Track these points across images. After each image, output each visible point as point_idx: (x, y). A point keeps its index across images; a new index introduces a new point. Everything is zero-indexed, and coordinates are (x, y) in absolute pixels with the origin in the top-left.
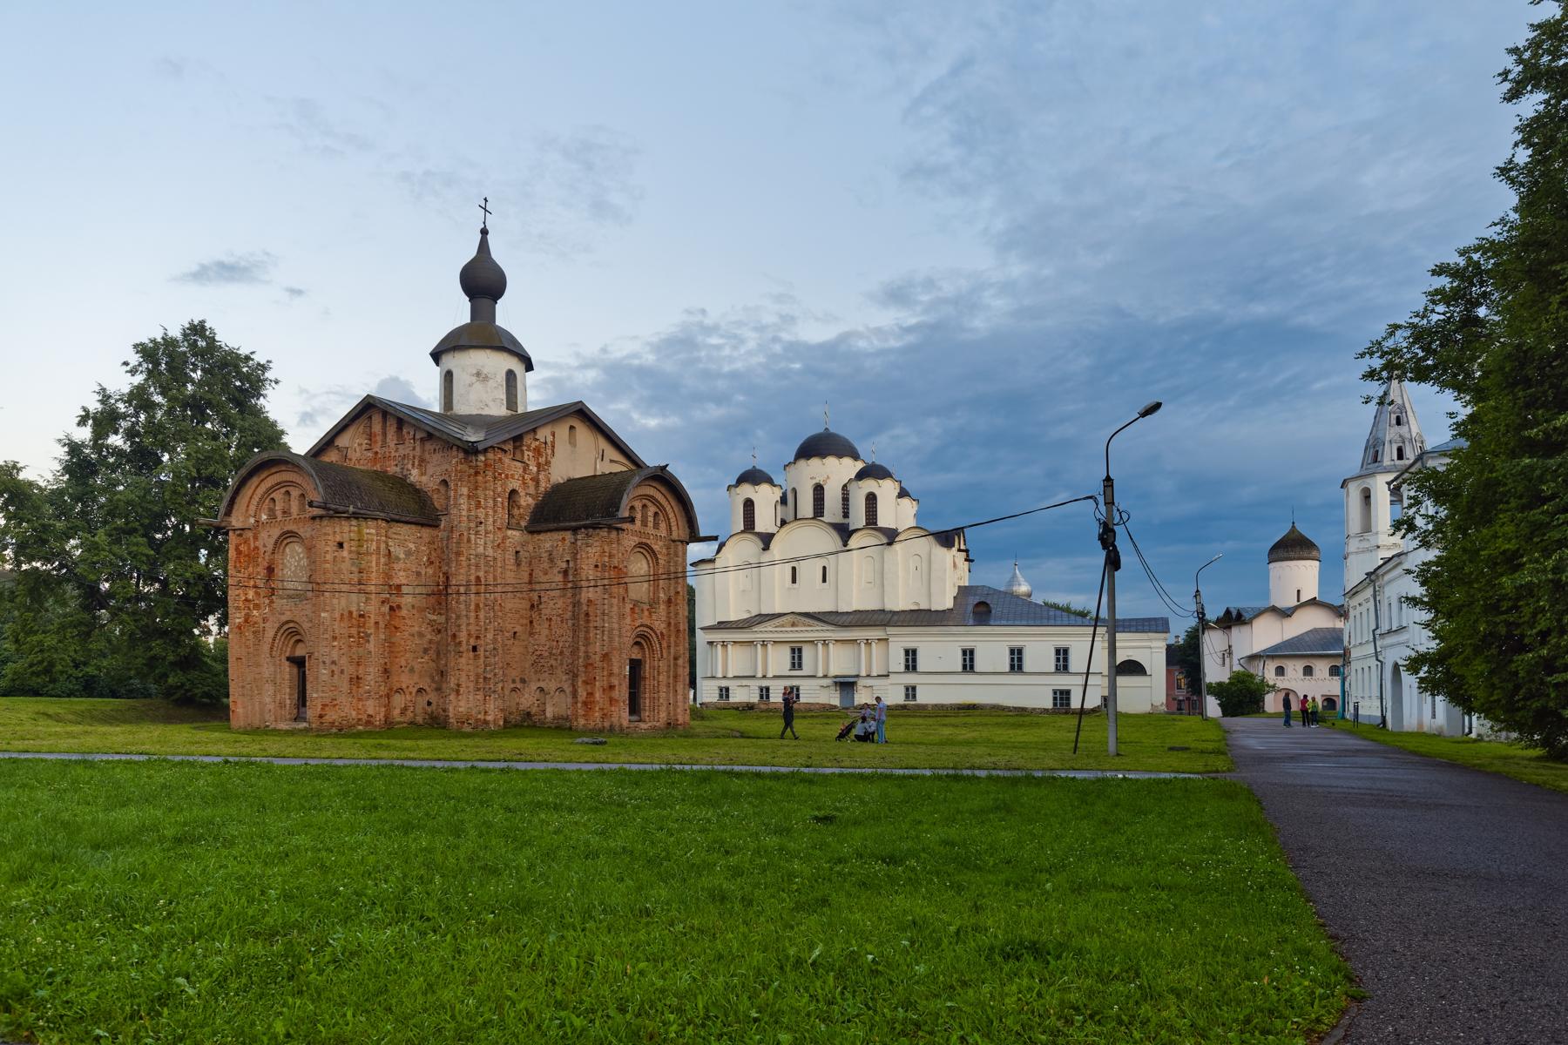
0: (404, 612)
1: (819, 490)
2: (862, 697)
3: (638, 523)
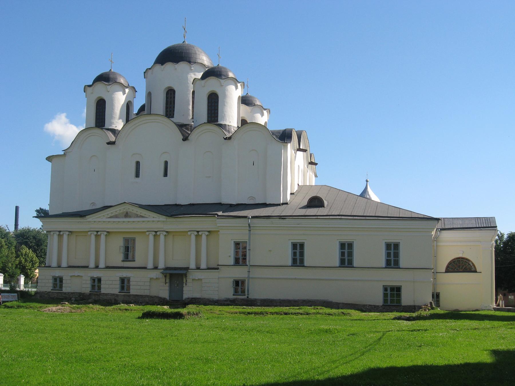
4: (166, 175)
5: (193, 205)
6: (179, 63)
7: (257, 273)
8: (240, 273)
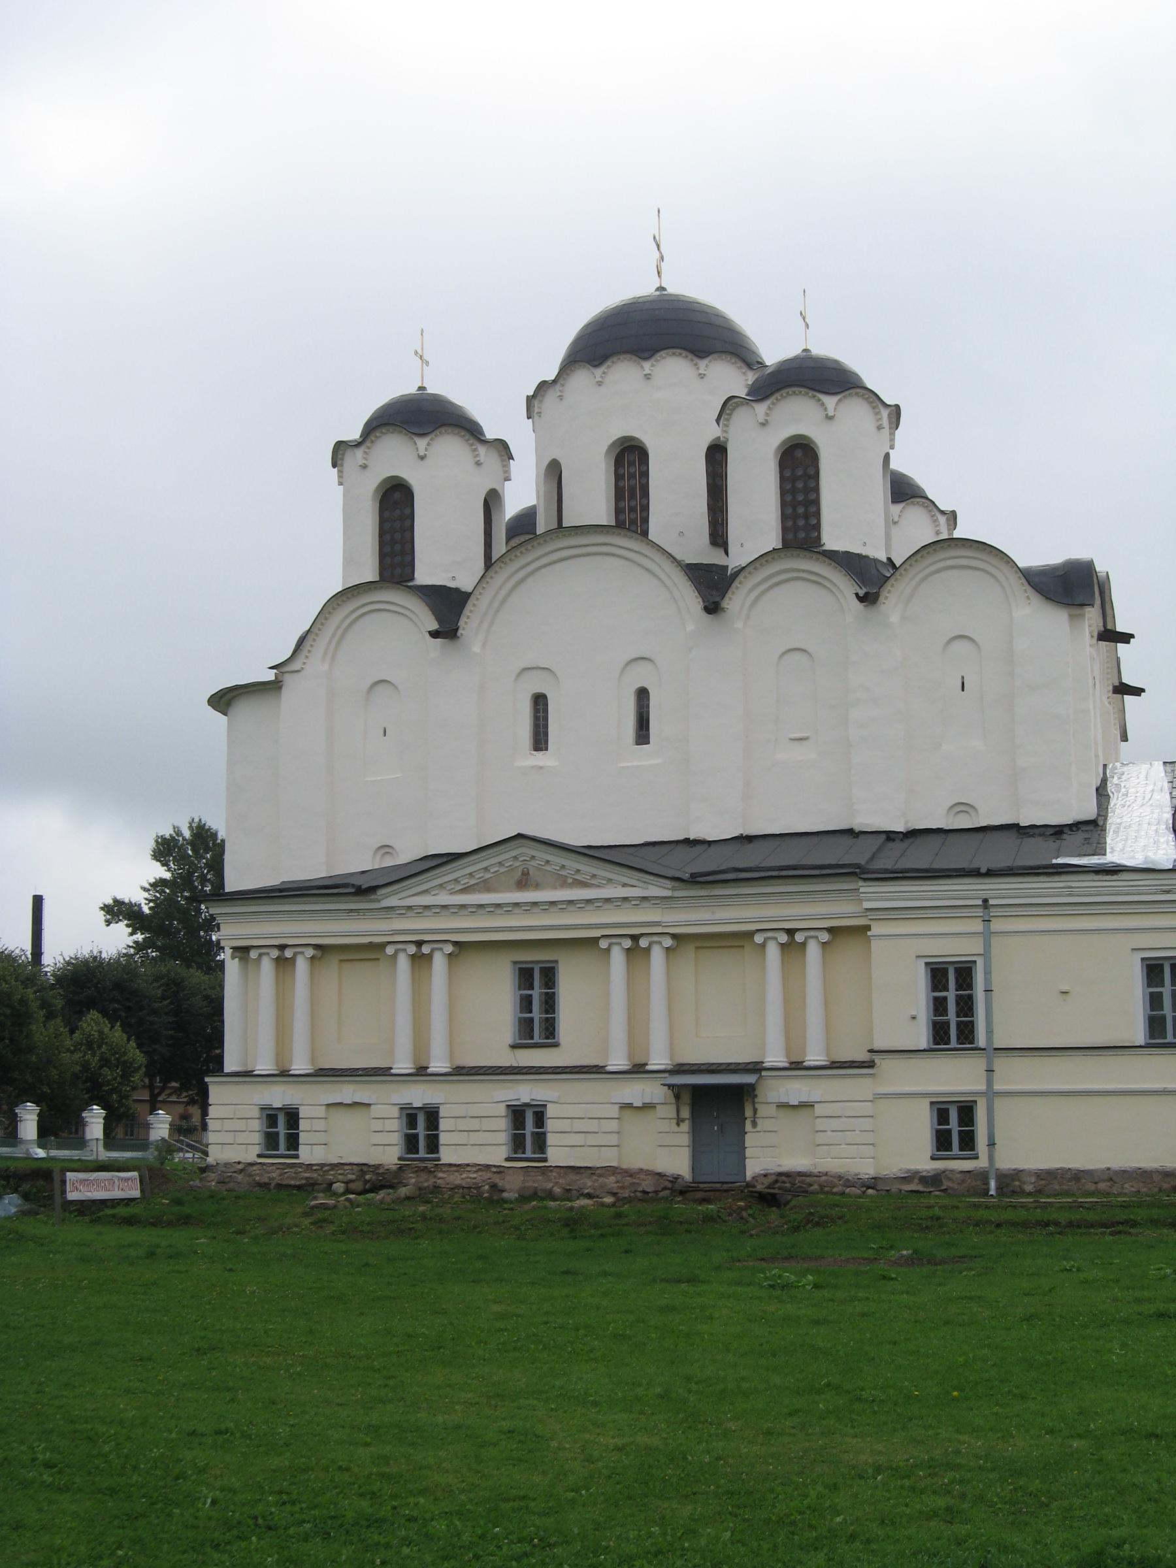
1: (630, 458)
2: (772, 1149)
5: (750, 839)
6: (657, 356)
7: (1014, 1075)
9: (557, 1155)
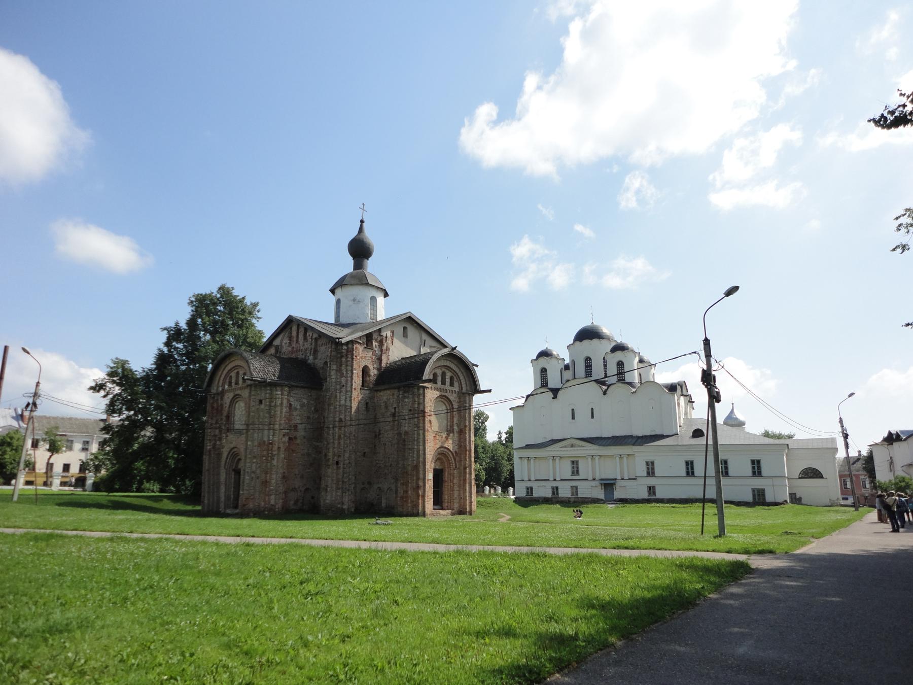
0: (298, 441)
1: (588, 360)
3: (439, 382)
4: (592, 417)
8: (651, 481)
9: (580, 495)
